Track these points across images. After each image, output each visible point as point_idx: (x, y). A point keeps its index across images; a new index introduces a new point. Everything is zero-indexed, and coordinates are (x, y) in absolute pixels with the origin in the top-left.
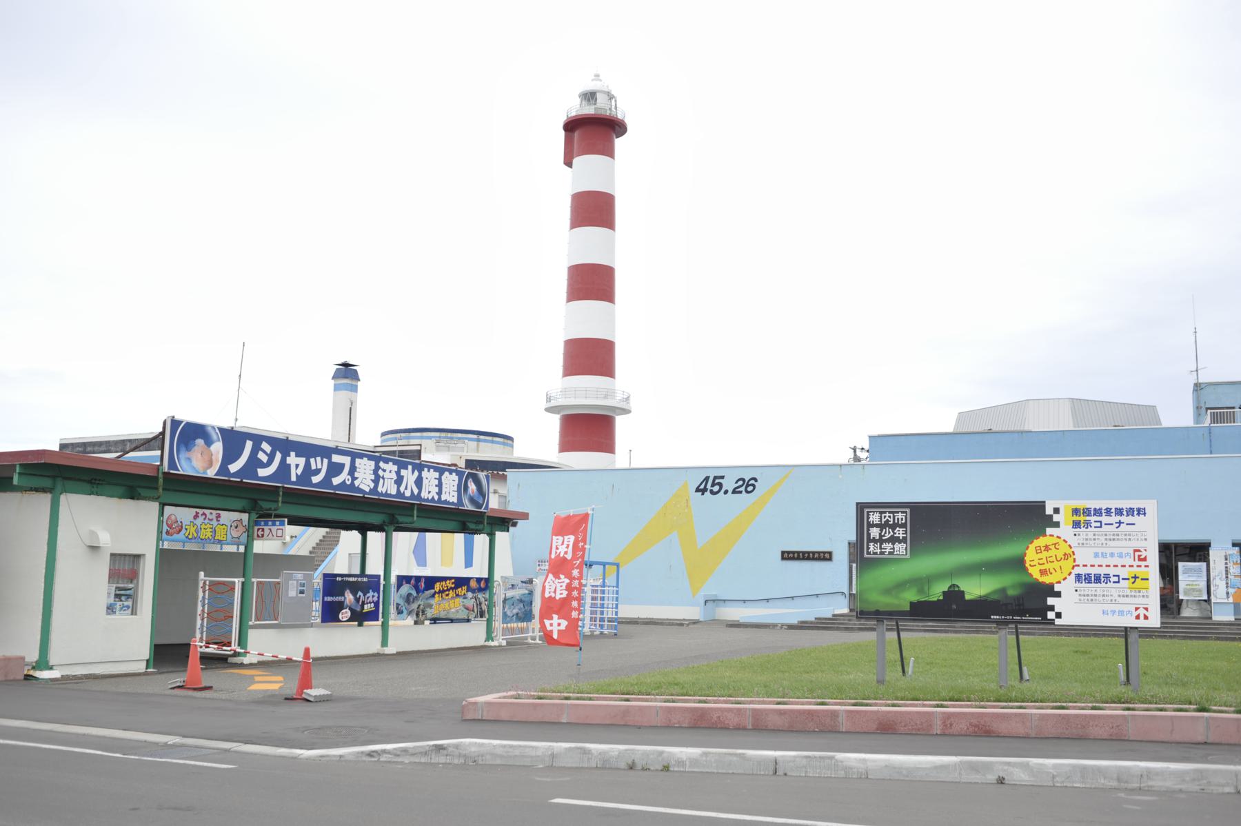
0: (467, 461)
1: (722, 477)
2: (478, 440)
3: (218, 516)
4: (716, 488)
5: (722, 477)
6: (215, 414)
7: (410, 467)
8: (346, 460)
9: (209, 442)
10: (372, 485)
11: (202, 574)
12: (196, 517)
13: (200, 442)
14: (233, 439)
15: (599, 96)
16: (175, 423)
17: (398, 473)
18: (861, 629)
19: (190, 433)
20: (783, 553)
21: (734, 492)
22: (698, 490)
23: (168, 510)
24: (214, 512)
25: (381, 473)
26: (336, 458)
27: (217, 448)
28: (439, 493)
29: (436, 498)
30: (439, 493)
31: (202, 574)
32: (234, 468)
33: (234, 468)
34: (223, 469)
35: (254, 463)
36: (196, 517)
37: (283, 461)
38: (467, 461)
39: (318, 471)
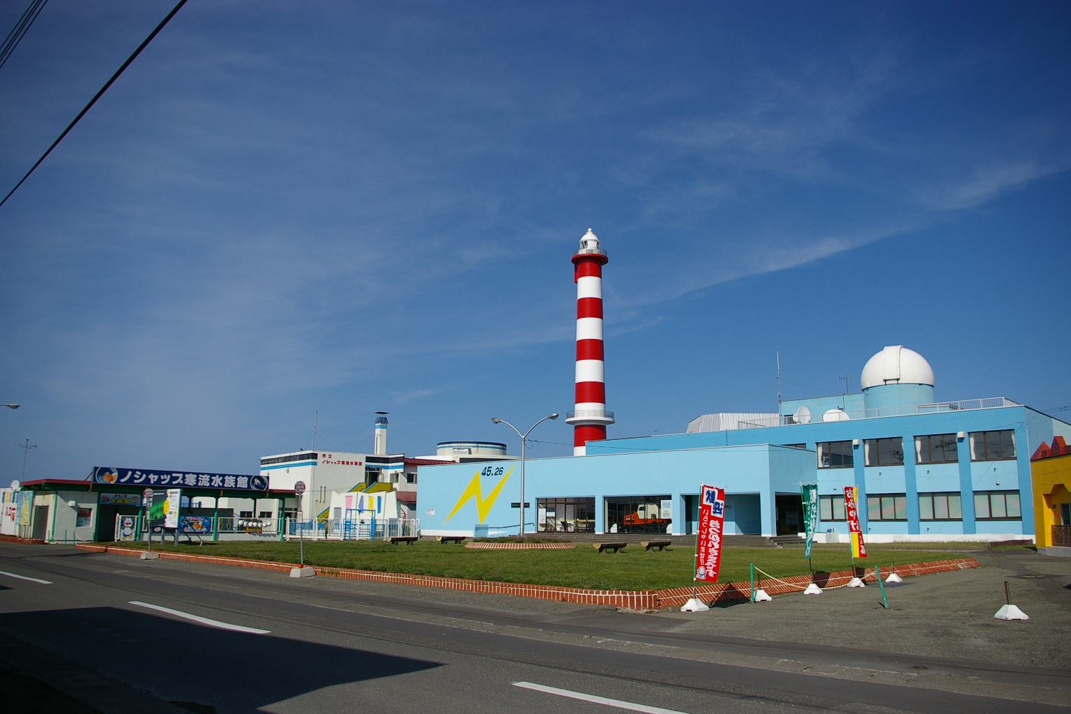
0: (461, 459)
1: (491, 467)
2: (477, 447)
3: (126, 496)
4: (489, 473)
5: (491, 467)
6: (115, 463)
7: (217, 476)
8: (181, 476)
9: (111, 473)
10: (195, 483)
11: (118, 514)
12: (116, 496)
13: (108, 473)
14: (122, 472)
15: (588, 242)
16: (96, 468)
17: (210, 478)
18: (238, 533)
19: (104, 471)
20: (512, 504)
21: (495, 474)
22: (483, 474)
23: (102, 494)
24: (124, 495)
25: (200, 479)
26: (174, 475)
27: (115, 474)
28: (236, 484)
29: (234, 486)
30: (236, 484)
31: (118, 514)
32: (122, 480)
33: (122, 480)
34: (118, 481)
35: (132, 478)
36: (116, 496)
37: (147, 477)
38: (461, 459)
39: (165, 480)
